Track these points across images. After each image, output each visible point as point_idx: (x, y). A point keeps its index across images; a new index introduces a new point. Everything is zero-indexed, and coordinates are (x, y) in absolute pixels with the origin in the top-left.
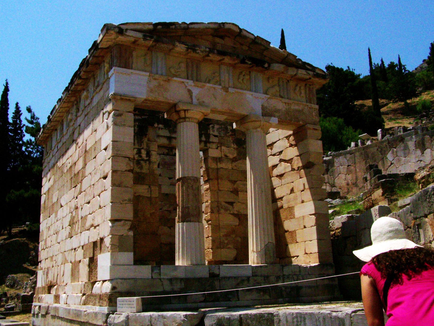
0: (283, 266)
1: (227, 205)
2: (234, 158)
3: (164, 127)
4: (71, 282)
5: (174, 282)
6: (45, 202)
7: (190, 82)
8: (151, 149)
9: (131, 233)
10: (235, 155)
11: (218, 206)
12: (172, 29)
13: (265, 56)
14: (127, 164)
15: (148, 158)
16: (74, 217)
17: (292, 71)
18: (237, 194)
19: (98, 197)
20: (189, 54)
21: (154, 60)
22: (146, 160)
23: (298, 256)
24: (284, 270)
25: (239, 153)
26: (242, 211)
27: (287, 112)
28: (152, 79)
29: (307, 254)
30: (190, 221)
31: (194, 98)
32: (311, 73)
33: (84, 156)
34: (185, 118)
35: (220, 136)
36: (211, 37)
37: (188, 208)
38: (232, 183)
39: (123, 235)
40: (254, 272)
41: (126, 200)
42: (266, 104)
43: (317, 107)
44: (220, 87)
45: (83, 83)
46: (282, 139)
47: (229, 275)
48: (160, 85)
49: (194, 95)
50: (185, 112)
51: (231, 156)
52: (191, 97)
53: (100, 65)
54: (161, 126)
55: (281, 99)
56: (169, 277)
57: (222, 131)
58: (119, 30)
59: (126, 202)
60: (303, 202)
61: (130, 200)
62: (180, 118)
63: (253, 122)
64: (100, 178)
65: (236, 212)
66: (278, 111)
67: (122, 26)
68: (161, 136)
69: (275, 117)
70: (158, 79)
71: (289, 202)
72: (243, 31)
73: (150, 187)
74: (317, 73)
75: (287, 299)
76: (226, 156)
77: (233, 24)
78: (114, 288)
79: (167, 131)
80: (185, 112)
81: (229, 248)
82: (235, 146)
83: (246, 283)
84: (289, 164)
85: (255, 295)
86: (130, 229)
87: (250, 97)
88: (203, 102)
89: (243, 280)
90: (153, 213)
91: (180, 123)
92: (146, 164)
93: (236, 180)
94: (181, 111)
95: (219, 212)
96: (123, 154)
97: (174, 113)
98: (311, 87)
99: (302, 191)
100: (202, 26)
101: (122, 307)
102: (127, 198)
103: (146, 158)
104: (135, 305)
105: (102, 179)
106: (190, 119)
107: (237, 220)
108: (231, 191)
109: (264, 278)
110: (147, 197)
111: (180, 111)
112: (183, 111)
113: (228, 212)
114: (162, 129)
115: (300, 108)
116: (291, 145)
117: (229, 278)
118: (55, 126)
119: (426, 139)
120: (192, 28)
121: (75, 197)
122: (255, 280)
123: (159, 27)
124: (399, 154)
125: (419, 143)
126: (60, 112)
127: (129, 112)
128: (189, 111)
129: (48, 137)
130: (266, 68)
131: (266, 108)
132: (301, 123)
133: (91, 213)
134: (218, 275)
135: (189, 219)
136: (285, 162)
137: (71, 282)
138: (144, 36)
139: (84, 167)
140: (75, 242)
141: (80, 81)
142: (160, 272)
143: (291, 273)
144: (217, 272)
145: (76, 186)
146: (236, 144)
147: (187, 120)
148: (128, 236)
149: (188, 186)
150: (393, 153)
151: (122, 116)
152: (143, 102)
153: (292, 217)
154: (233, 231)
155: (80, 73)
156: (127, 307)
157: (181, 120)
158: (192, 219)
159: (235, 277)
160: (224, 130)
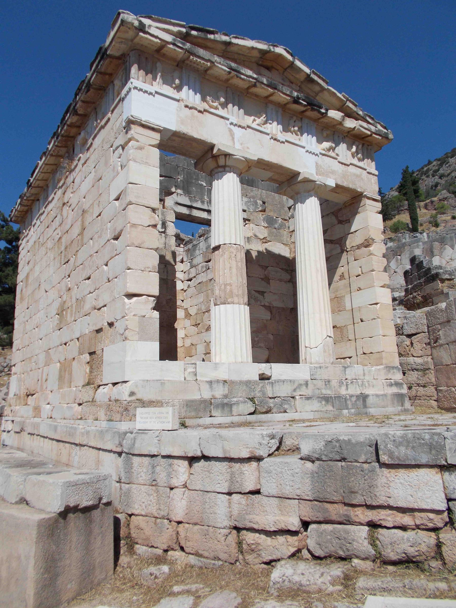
0: (345, 368)
1: (257, 295)
3: (183, 192)
4: (59, 388)
5: (215, 385)
6: (22, 291)
9: (156, 314)
10: (266, 235)
12: (210, 40)
15: (163, 230)
16: (65, 302)
17: (350, 123)
18: (269, 283)
19: (104, 266)
20: (230, 81)
22: (162, 232)
23: (350, 358)
24: (347, 373)
25: (270, 234)
28: (183, 106)
29: (364, 354)
30: (233, 303)
31: (236, 140)
32: (373, 128)
33: (80, 219)
34: (224, 167)
35: (249, 211)
37: (230, 285)
38: (263, 268)
39: (144, 316)
40: (313, 375)
41: (148, 268)
42: (320, 162)
43: (377, 173)
45: (78, 124)
46: (328, 215)
47: (283, 378)
49: (236, 137)
50: (226, 158)
52: (233, 139)
53: (105, 90)
54: (179, 191)
55: (337, 157)
56: (208, 379)
57: (251, 206)
58: (139, 24)
59: (149, 270)
60: (360, 289)
61: (154, 267)
62: (219, 167)
63: (306, 183)
64: (108, 240)
65: (267, 304)
66: (333, 172)
69: (331, 178)
70: (191, 108)
71: (337, 291)
73: (166, 266)
74: (379, 130)
75: (353, 411)
76: (255, 236)
78: (132, 394)
79: (187, 198)
80: (226, 158)
81: (260, 347)
82: (266, 225)
83: (304, 387)
84: (338, 245)
85: (316, 405)
86: (154, 309)
87: (304, 150)
88: (248, 148)
89: (301, 385)
90: (170, 299)
91: (216, 173)
92: (161, 238)
93: (267, 265)
94: (220, 157)
97: (211, 159)
98: (370, 147)
99: (357, 276)
101: (145, 422)
104: (170, 419)
105: (112, 241)
106: (232, 169)
107: (269, 314)
109: (325, 382)
111: (219, 156)
112: (223, 157)
113: (259, 302)
114: (181, 195)
116: (340, 222)
117: (284, 381)
118: (36, 194)
119: (434, 246)
120: (235, 44)
121: (67, 275)
122: (315, 385)
123: (194, 33)
124: (403, 262)
125: (426, 250)
126: (45, 173)
127: (153, 146)
128: (230, 156)
129: (27, 212)
130: (323, 113)
132: (359, 190)
133: (91, 292)
134: (269, 378)
136: (332, 243)
137: (59, 388)
138: (174, 40)
139: (81, 234)
140: (65, 335)
141: (75, 119)
142: (196, 371)
143: (354, 377)
144: (268, 373)
145: (69, 260)
146: (267, 223)
147: (227, 169)
148: (151, 318)
149: (230, 256)
150: (397, 260)
151: (143, 150)
152: (169, 139)
153: (341, 309)
154: (265, 327)
155: (76, 105)
156: (155, 422)
157: (220, 169)
158: (236, 300)
159: (291, 381)
160: (253, 205)
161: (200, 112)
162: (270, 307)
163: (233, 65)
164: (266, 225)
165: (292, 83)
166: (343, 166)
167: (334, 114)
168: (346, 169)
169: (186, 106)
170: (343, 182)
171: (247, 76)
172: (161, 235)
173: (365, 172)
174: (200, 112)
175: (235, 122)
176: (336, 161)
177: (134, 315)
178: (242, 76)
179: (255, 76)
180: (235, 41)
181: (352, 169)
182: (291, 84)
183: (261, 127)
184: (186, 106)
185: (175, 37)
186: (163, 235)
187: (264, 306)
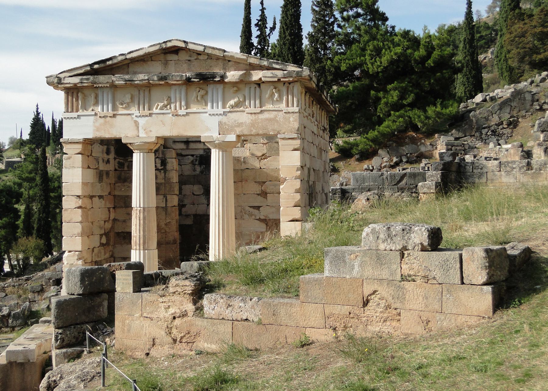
1: (251, 210)
2: (263, 155)
7: (137, 113)
8: (167, 156)
10: (265, 152)
11: (241, 212)
13: (229, 61)
14: (77, 202)
21: (100, 98)
22: (161, 169)
26: (271, 217)
27: (253, 125)
31: (140, 128)
32: (280, 74)
36: (162, 55)
44: (169, 111)
48: (106, 122)
51: (259, 154)
52: (138, 128)
61: (78, 234)
65: (262, 217)
66: (240, 125)
67: (60, 76)
68: (178, 142)
72: (189, 44)
74: (290, 72)
77: (177, 40)
82: (266, 141)
86: (79, 259)
88: (151, 131)
95: (242, 218)
96: (73, 194)
100: (141, 53)
102: (76, 232)
103: (160, 168)
107: (265, 226)
108: (258, 194)
110: (163, 208)
113: (253, 217)
115: (272, 115)
131: (225, 123)
135: (135, 247)
138: (81, 79)
146: (266, 139)
158: (138, 248)
161: (110, 117)
162: (265, 219)
163: (127, 77)
164: (266, 141)
165: (200, 54)
166: (253, 115)
167: (233, 75)
168: (257, 116)
169: (100, 117)
170: (251, 131)
171: (140, 81)
172: (160, 172)
173: (281, 113)
174: (110, 117)
175: (139, 115)
176: (245, 113)
177: (67, 264)
178: (136, 82)
179: (146, 78)
180: (129, 56)
181: (266, 115)
182: (200, 57)
183: (163, 109)
184: (100, 117)
185: (80, 77)
186: (162, 171)
187: (260, 220)
